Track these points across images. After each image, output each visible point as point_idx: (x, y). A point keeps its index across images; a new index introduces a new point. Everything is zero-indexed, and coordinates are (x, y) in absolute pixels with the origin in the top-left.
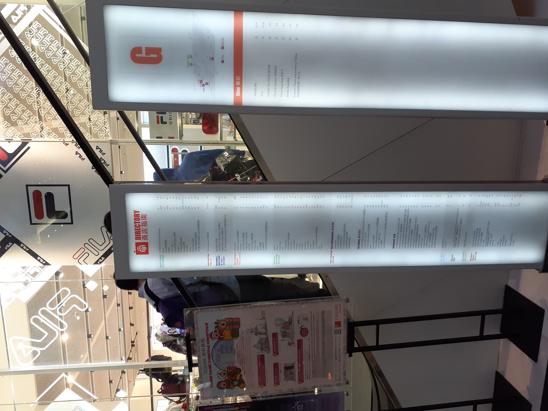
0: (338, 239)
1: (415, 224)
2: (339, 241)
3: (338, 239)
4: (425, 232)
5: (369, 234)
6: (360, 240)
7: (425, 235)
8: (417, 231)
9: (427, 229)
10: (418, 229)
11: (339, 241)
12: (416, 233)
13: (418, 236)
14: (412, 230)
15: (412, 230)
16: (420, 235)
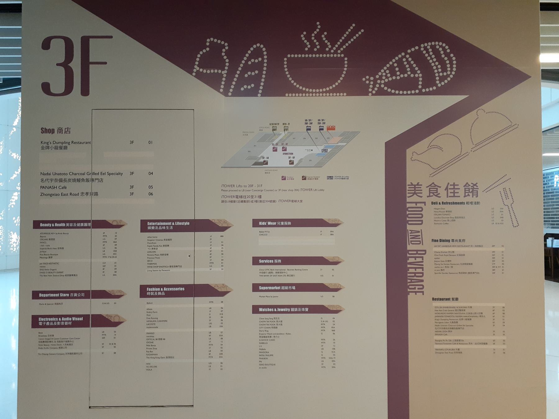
0: (447, 211)
1: (465, 326)
2: (444, 212)
3: (447, 211)
4: (455, 340)
5: (453, 255)
6: (449, 242)
7: (451, 341)
8: (457, 328)
9: (458, 342)
10: (459, 328)
11: (444, 212)
12: (454, 327)
13: (451, 330)
14: (457, 322)
15: (457, 322)
16: (451, 331)
